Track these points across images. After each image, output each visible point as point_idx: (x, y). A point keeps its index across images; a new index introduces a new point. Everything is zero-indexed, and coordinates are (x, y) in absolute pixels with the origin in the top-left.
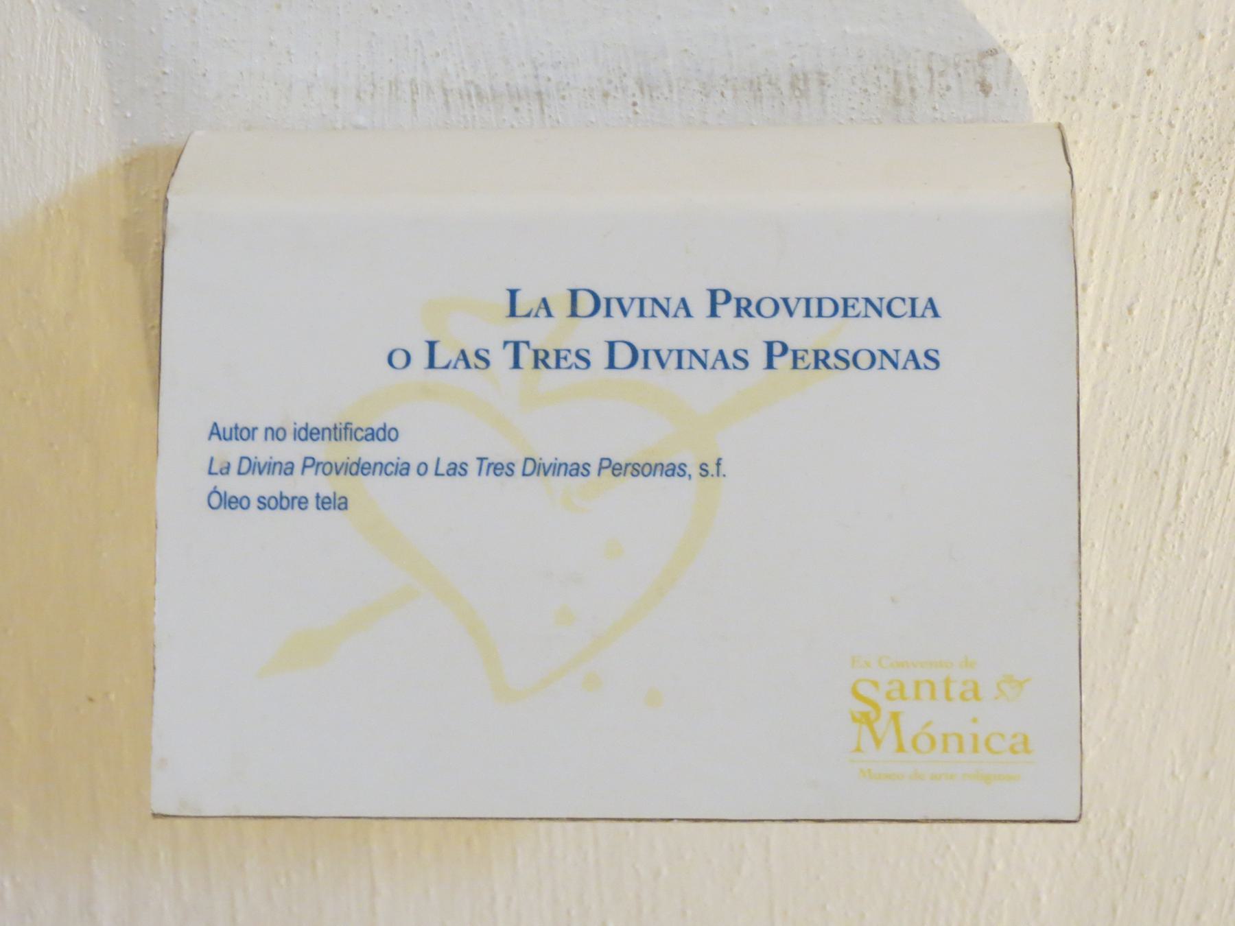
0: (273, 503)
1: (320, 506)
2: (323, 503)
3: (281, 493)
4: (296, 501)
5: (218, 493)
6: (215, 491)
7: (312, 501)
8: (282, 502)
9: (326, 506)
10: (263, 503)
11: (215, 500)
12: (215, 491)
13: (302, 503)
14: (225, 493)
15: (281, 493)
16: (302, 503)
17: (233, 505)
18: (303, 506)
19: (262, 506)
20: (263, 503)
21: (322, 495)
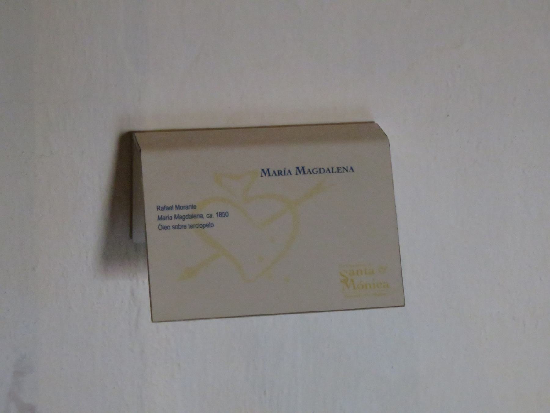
0: (177, 227)
1: (190, 227)
2: (191, 226)
3: (179, 225)
4: (183, 226)
5: (161, 225)
6: (160, 225)
7: (188, 226)
8: (179, 227)
9: (192, 227)
10: (174, 228)
11: (160, 227)
12: (160, 225)
13: (185, 227)
14: (163, 225)
15: (179, 225)
16: (185, 227)
17: (166, 229)
18: (185, 228)
19: (174, 228)
20: (174, 228)
21: (190, 224)
